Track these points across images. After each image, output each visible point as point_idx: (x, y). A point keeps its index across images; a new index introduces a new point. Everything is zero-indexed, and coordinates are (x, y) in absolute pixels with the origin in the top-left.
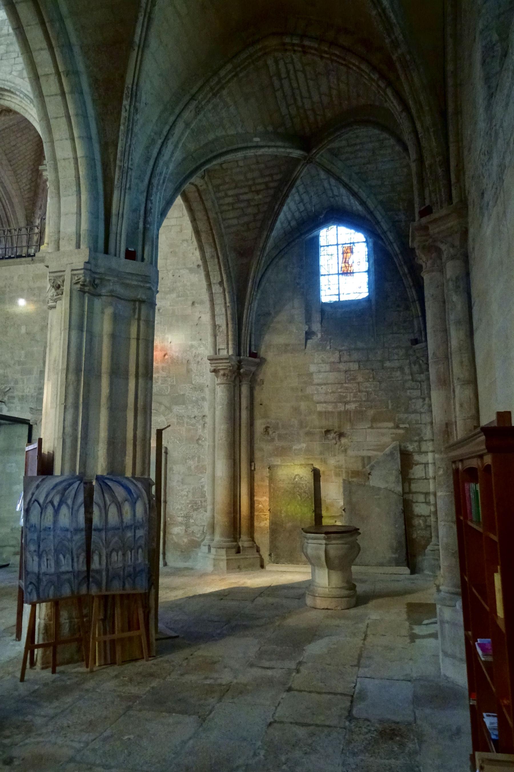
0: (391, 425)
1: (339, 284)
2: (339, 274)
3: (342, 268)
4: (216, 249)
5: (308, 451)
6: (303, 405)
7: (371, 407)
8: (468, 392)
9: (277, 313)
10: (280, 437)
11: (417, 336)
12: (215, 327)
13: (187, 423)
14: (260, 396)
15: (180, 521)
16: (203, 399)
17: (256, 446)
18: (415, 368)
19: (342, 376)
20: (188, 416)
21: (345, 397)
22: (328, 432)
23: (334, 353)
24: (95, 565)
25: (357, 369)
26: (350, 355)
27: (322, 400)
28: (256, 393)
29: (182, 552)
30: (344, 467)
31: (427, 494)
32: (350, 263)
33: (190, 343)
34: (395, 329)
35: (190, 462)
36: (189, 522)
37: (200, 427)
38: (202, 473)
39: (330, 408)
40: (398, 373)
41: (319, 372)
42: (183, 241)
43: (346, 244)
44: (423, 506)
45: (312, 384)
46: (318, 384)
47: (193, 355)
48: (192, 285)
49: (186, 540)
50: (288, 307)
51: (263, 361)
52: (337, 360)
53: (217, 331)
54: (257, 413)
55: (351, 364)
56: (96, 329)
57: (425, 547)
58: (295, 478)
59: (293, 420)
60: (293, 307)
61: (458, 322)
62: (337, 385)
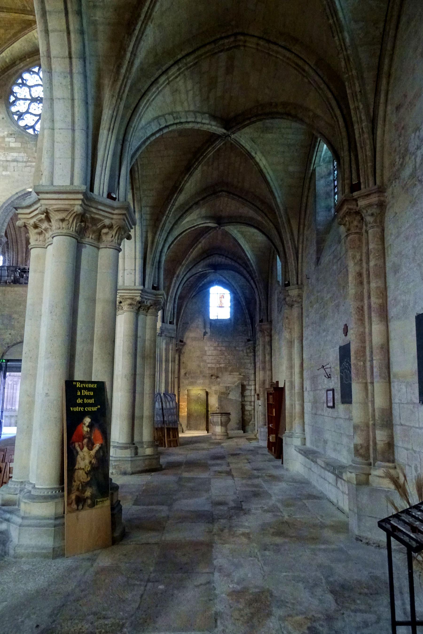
0: (238, 374)
5: (203, 384)
6: (202, 364)
7: (230, 366)
8: (270, 373)
9: (192, 323)
10: (192, 377)
11: (250, 338)
14: (183, 359)
17: (181, 381)
18: (248, 351)
22: (212, 376)
24: (165, 419)
28: (181, 357)
31: (251, 402)
34: (241, 334)
39: (213, 366)
40: (241, 353)
44: (249, 406)
50: (197, 321)
51: (185, 344)
54: (182, 367)
56: (161, 347)
57: (249, 422)
61: (268, 354)
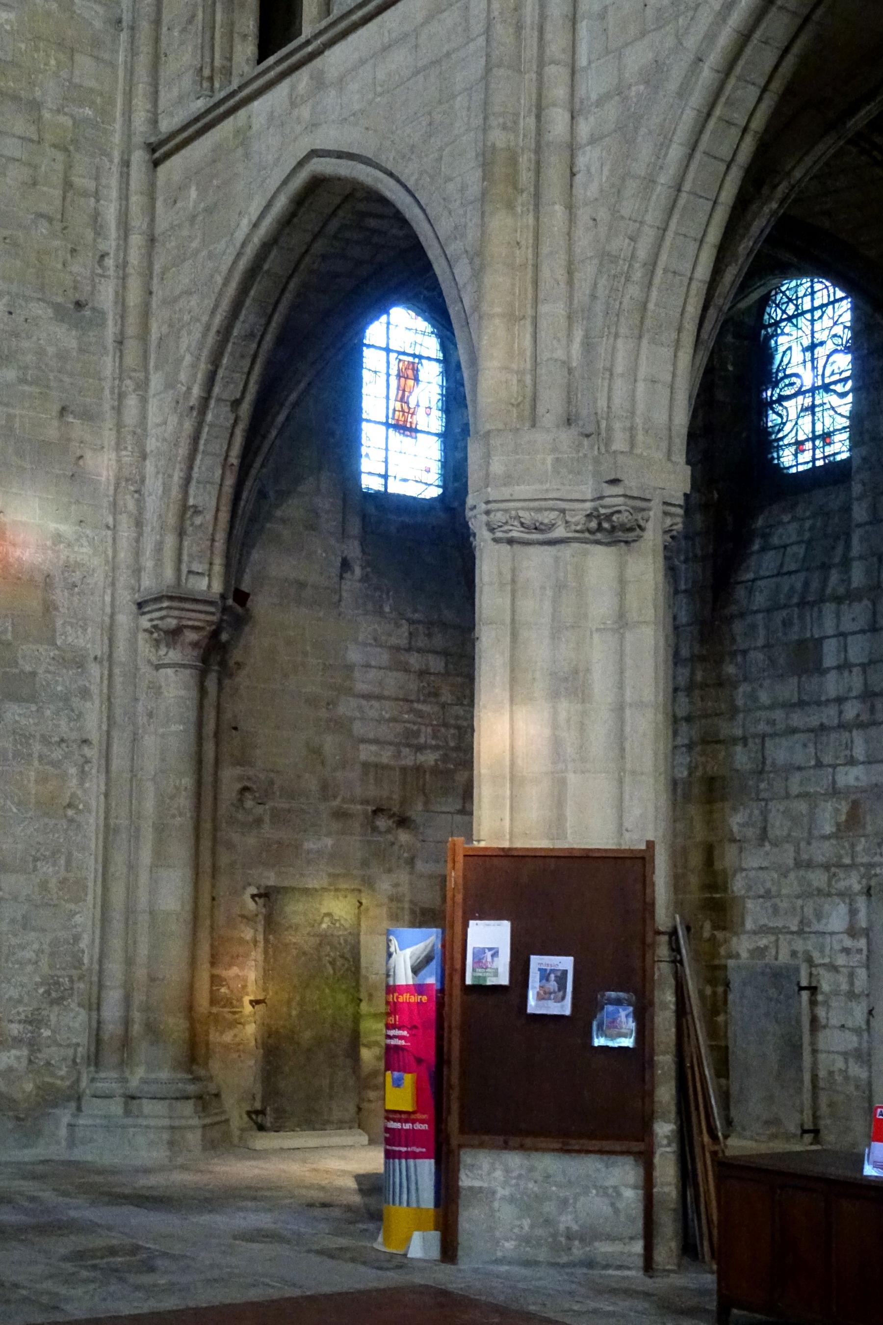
1: (387, 449)
2: (387, 425)
3: (394, 410)
4: (269, 322)
6: (329, 743)
10: (277, 817)
12: (185, 510)
13: (41, 757)
15: (15, 1033)
16: (85, 693)
19: (413, 685)
20: (43, 736)
21: (416, 735)
23: (398, 626)
25: (443, 671)
26: (429, 635)
27: (371, 736)
29: (18, 1119)
30: (407, 899)
32: (412, 404)
33: (53, 526)
35: (45, 869)
36: (40, 1035)
37: (73, 771)
38: (77, 900)
39: (386, 756)
41: (368, 666)
42: (41, 215)
43: (404, 353)
45: (350, 692)
46: (367, 697)
47: (61, 562)
48: (63, 356)
49: (29, 1087)
52: (403, 642)
53: (188, 522)
55: (431, 657)
58: (321, 923)
59: (307, 775)
60: (318, 490)
62: (401, 703)
